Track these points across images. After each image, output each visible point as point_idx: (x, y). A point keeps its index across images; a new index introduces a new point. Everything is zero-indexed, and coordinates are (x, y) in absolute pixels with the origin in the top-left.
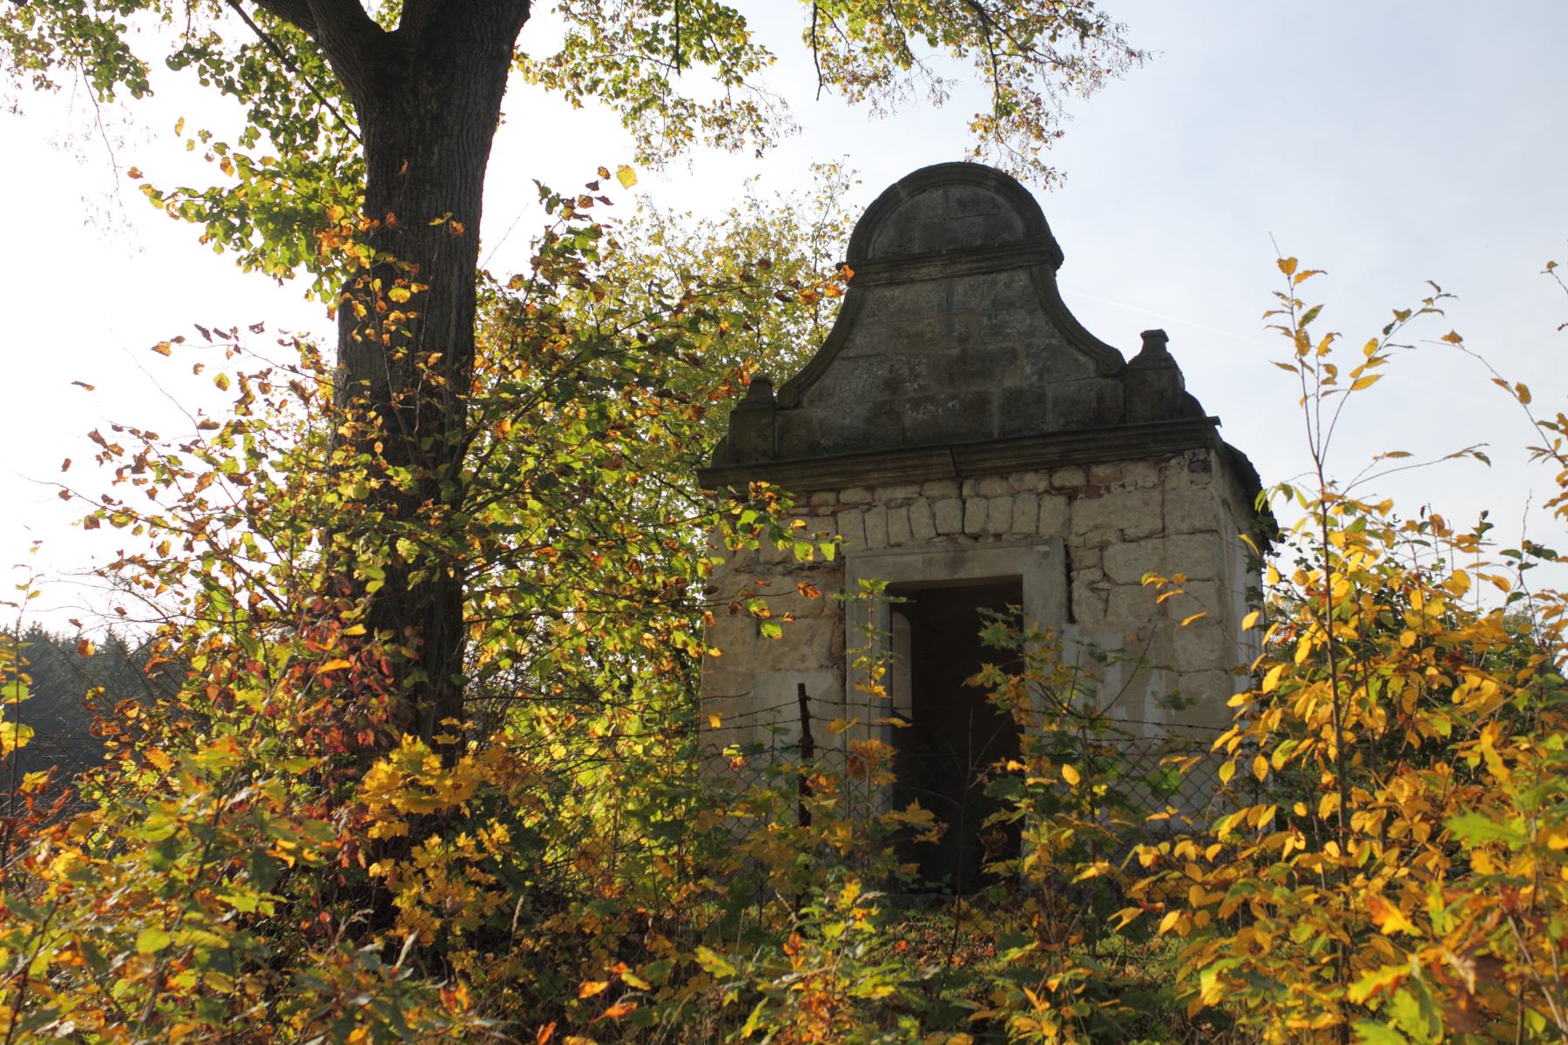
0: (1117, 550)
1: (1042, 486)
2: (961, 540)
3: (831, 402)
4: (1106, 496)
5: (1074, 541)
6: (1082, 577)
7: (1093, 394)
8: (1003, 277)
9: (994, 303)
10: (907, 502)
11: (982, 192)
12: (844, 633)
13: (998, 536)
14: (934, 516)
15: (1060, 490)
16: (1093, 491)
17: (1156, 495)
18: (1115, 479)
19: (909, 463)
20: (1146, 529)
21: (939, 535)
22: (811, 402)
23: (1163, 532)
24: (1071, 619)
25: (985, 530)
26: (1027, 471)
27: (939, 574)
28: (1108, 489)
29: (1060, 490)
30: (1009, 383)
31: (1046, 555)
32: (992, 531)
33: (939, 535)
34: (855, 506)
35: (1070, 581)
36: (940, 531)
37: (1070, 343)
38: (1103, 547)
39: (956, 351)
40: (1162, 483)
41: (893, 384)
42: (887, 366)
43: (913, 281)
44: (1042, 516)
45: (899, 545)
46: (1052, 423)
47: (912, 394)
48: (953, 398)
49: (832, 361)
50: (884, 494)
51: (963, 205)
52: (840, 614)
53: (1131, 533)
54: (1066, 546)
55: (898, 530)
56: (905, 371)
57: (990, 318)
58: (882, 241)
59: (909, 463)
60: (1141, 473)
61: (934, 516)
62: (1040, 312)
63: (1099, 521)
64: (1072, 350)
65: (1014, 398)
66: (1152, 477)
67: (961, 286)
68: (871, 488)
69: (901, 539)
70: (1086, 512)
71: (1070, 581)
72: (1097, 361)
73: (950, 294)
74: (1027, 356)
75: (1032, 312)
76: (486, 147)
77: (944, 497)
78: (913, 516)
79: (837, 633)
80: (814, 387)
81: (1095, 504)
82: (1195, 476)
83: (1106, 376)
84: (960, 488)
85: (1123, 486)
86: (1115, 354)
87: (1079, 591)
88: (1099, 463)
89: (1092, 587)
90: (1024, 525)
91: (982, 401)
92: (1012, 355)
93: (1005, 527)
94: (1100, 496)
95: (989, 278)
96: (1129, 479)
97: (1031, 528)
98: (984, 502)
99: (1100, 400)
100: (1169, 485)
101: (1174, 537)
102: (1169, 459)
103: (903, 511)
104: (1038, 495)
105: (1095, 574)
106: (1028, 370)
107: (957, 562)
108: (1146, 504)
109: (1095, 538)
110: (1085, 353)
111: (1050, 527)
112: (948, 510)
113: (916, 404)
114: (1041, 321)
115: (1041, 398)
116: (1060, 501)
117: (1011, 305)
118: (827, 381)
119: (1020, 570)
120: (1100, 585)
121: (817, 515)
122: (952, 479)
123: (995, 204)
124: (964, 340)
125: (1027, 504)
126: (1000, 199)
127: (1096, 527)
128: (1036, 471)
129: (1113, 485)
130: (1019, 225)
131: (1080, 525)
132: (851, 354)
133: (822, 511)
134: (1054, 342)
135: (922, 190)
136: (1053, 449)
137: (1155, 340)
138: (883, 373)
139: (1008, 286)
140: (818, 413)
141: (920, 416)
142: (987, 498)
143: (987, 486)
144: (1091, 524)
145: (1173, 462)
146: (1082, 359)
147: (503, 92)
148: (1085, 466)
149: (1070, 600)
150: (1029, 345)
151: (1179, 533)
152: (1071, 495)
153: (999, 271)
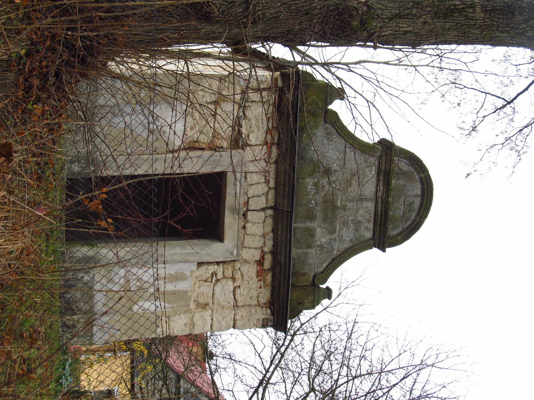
0: (230, 285)
1: (266, 249)
2: (245, 209)
3: (325, 140)
4: (257, 279)
5: (238, 265)
6: (219, 270)
7: (307, 270)
8: (371, 226)
9: (360, 222)
10: (267, 182)
11: (414, 215)
12: (203, 149)
13: (244, 227)
14: (258, 196)
15: (263, 257)
16: (259, 274)
17: (255, 302)
18: (264, 283)
19: (287, 189)
20: (238, 297)
21: (248, 198)
22: (326, 129)
23: (236, 306)
24: (200, 264)
25: (248, 221)
26: (274, 242)
27: (229, 201)
28: (260, 280)
29: (263, 257)
30: (318, 230)
31: (232, 254)
32: (247, 225)
33: (248, 198)
34: (269, 156)
35: (218, 263)
36: (250, 200)
37: (333, 260)
38: (233, 279)
39: (339, 204)
40: (259, 305)
41: (328, 172)
42: (338, 169)
43: (378, 181)
44: (251, 250)
45: (245, 177)
46: (295, 252)
47: (321, 182)
48: (316, 203)
49: (345, 140)
50: (272, 169)
51: (410, 205)
52: (214, 148)
53: (238, 291)
54: (235, 261)
55: (254, 178)
56: (333, 178)
57: (352, 220)
59: (287, 189)
60: (265, 295)
61: (258, 196)
62: (350, 244)
63: (245, 277)
64: (330, 260)
65: (311, 233)
66: (262, 300)
67: (370, 205)
68: (276, 162)
69: (249, 180)
70: (251, 270)
71: (218, 263)
72: (322, 273)
73: (367, 200)
74: (330, 239)
75: (351, 241)
76: (367, 250)
77: (267, 200)
78: (260, 186)
79: (204, 146)
80: (333, 130)
81: (254, 275)
82: (261, 321)
83: (314, 277)
84: (271, 208)
85: (261, 287)
86: (325, 281)
87: (213, 268)
88: (273, 276)
89: (214, 274)
90: (248, 241)
91: (311, 217)
92: (332, 232)
93: (248, 232)
94: (257, 277)
95: (372, 219)
96: (263, 289)
97: (246, 244)
98: (262, 221)
99: (303, 274)
100: (259, 309)
101: (234, 312)
102: (271, 309)
103: (263, 180)
104: (262, 247)
105: (220, 276)
106: (323, 240)
107: (235, 210)
108: (251, 298)
109: (238, 275)
110: (327, 267)
111: (246, 254)
112: (262, 202)
113: (316, 185)
114: (347, 245)
115: (309, 246)
116: (258, 258)
117: (357, 230)
118: (335, 137)
119: (226, 241)
120: (214, 279)
121: (267, 134)
122: (275, 205)
123: (407, 220)
124: (344, 208)
125: (258, 243)
126: (409, 223)
127: (242, 275)
128: (273, 246)
129: (262, 283)
130: (395, 232)
131: (245, 268)
132: (347, 149)
133: (269, 136)
134: (335, 252)
135: (422, 183)
136: (283, 260)
137: (328, 293)
138: (335, 167)
139: (366, 228)
140: (320, 133)
141: (309, 187)
142: (264, 221)
143: (269, 221)
144: (244, 273)
145: (269, 311)
146: (324, 266)
147: (422, 162)
148: (273, 268)
149: (208, 263)
150: (336, 240)
151: (235, 315)
152: (260, 263)
153: (375, 224)
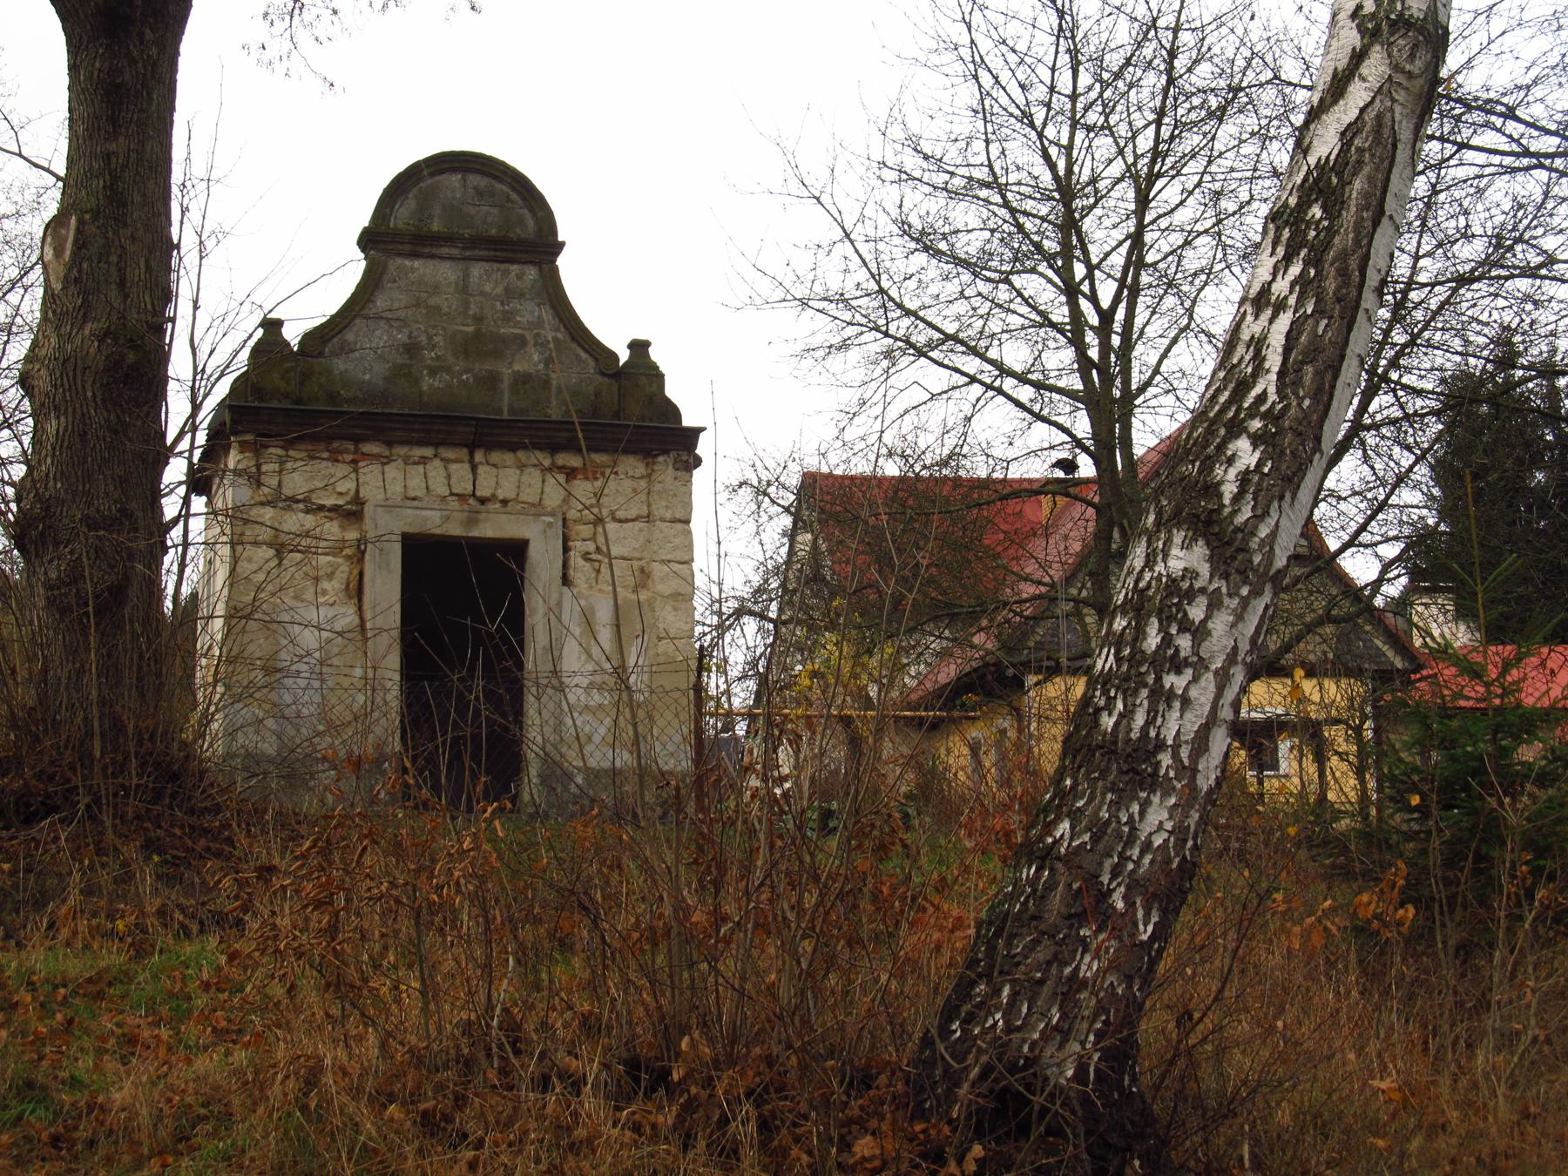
1: (547, 463)
2: (471, 501)
6: (578, 546)
7: (591, 388)
8: (515, 268)
9: (507, 290)
10: (423, 461)
11: (499, 186)
12: (361, 574)
13: (505, 502)
14: (449, 477)
15: (561, 469)
16: (589, 473)
17: (643, 483)
20: (633, 513)
21: (452, 494)
23: (648, 518)
24: (566, 580)
27: (454, 529)
29: (561, 469)
30: (517, 367)
31: (550, 525)
32: (501, 497)
33: (452, 494)
34: (377, 457)
35: (566, 550)
37: (573, 339)
39: (470, 329)
40: (649, 476)
41: (411, 349)
43: (432, 257)
44: (546, 489)
45: (414, 499)
48: (467, 371)
50: (402, 450)
51: (479, 193)
54: (564, 520)
55: (416, 484)
56: (423, 339)
58: (403, 215)
60: (632, 465)
61: (449, 477)
64: (574, 345)
65: (522, 380)
66: (641, 469)
67: (477, 270)
69: (419, 494)
71: (566, 550)
72: (597, 360)
73: (466, 276)
74: (536, 344)
78: (430, 474)
79: (356, 572)
83: (603, 374)
84: (472, 455)
86: (613, 356)
87: (576, 559)
89: (586, 557)
90: (529, 495)
91: (493, 380)
92: (522, 342)
93: (513, 496)
95: (503, 266)
96: (620, 469)
99: (597, 394)
103: (421, 468)
107: (472, 521)
110: (586, 351)
112: (461, 471)
113: (433, 372)
114: (547, 315)
115: (546, 384)
116: (561, 478)
117: (521, 296)
118: (350, 336)
120: (594, 556)
122: (466, 446)
123: (509, 199)
124: (479, 319)
125: (533, 477)
126: (514, 196)
128: (541, 449)
129: (608, 471)
130: (530, 223)
134: (560, 336)
135: (442, 172)
137: (639, 348)
139: (520, 277)
140: (340, 365)
141: (436, 384)
142: (495, 466)
143: (495, 456)
145: (661, 459)
146: (584, 355)
149: (565, 566)
150: (538, 335)
151: (663, 520)
153: (512, 261)
